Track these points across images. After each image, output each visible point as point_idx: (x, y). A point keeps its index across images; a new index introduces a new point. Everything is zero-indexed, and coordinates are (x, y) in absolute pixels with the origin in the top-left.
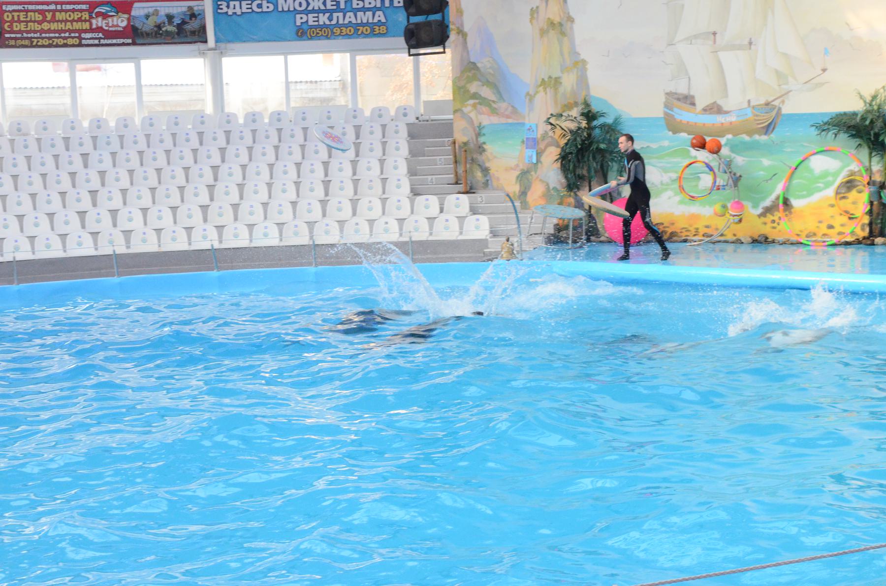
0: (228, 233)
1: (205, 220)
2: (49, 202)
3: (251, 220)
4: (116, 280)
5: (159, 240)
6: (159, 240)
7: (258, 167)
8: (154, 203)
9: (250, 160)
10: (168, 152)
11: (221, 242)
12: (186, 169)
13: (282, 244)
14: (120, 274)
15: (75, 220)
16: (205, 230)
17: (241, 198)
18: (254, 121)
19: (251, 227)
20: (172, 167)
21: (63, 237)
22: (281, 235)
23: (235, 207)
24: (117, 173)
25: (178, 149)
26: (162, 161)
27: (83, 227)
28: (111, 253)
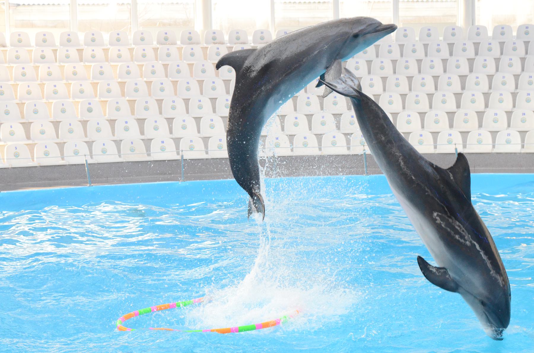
0: (470, 138)
1: (451, 126)
2: (308, 104)
3: (495, 127)
7: (504, 77)
8: (404, 108)
9: (497, 70)
10: (419, 61)
11: (465, 146)
12: (436, 78)
13: (524, 151)
14: (368, 174)
15: (331, 121)
16: (450, 135)
17: (487, 106)
18: (503, 34)
19: (494, 133)
20: (422, 76)
21: (319, 137)
22: (523, 141)
23: (480, 114)
24: (371, 80)
25: (429, 58)
26: (413, 70)
27: (338, 127)
28: (362, 153)
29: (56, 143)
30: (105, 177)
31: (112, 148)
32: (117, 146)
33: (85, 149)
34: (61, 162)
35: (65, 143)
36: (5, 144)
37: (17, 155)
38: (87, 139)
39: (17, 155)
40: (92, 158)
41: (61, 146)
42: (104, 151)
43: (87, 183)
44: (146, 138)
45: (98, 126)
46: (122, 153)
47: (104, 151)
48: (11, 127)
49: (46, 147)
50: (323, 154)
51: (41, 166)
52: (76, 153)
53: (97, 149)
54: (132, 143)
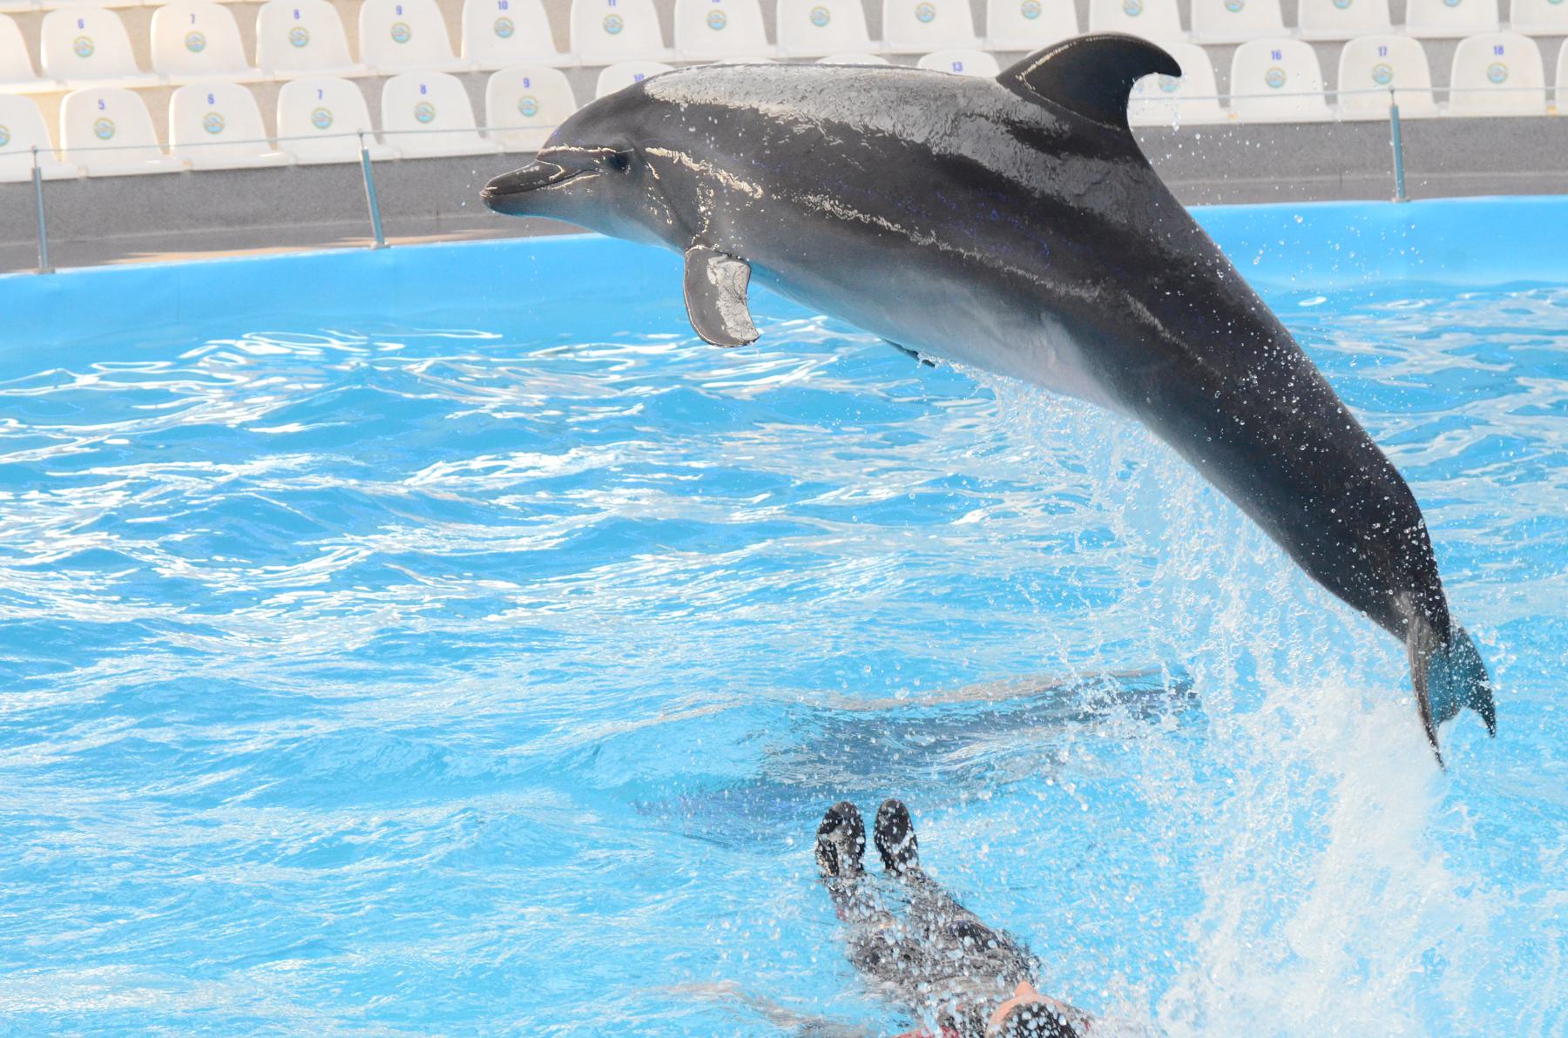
4: (1394, 210)
5: (1550, 78)
6: (1550, 78)
14: (1408, 194)
28: (1383, 113)
29: (249, 85)
30: (429, 212)
31: (453, 103)
32: (470, 94)
33: (351, 109)
34: (267, 157)
35: (279, 84)
36: (62, 88)
37: (104, 131)
38: (360, 70)
39: (104, 131)
40: (379, 137)
41: (267, 94)
42: (424, 114)
43: (365, 232)
44: (576, 63)
45: (401, 19)
46: (490, 123)
47: (424, 114)
48: (81, 24)
49: (211, 100)
50: (1234, 121)
51: (193, 172)
52: (322, 120)
53: (397, 104)
54: (527, 83)
